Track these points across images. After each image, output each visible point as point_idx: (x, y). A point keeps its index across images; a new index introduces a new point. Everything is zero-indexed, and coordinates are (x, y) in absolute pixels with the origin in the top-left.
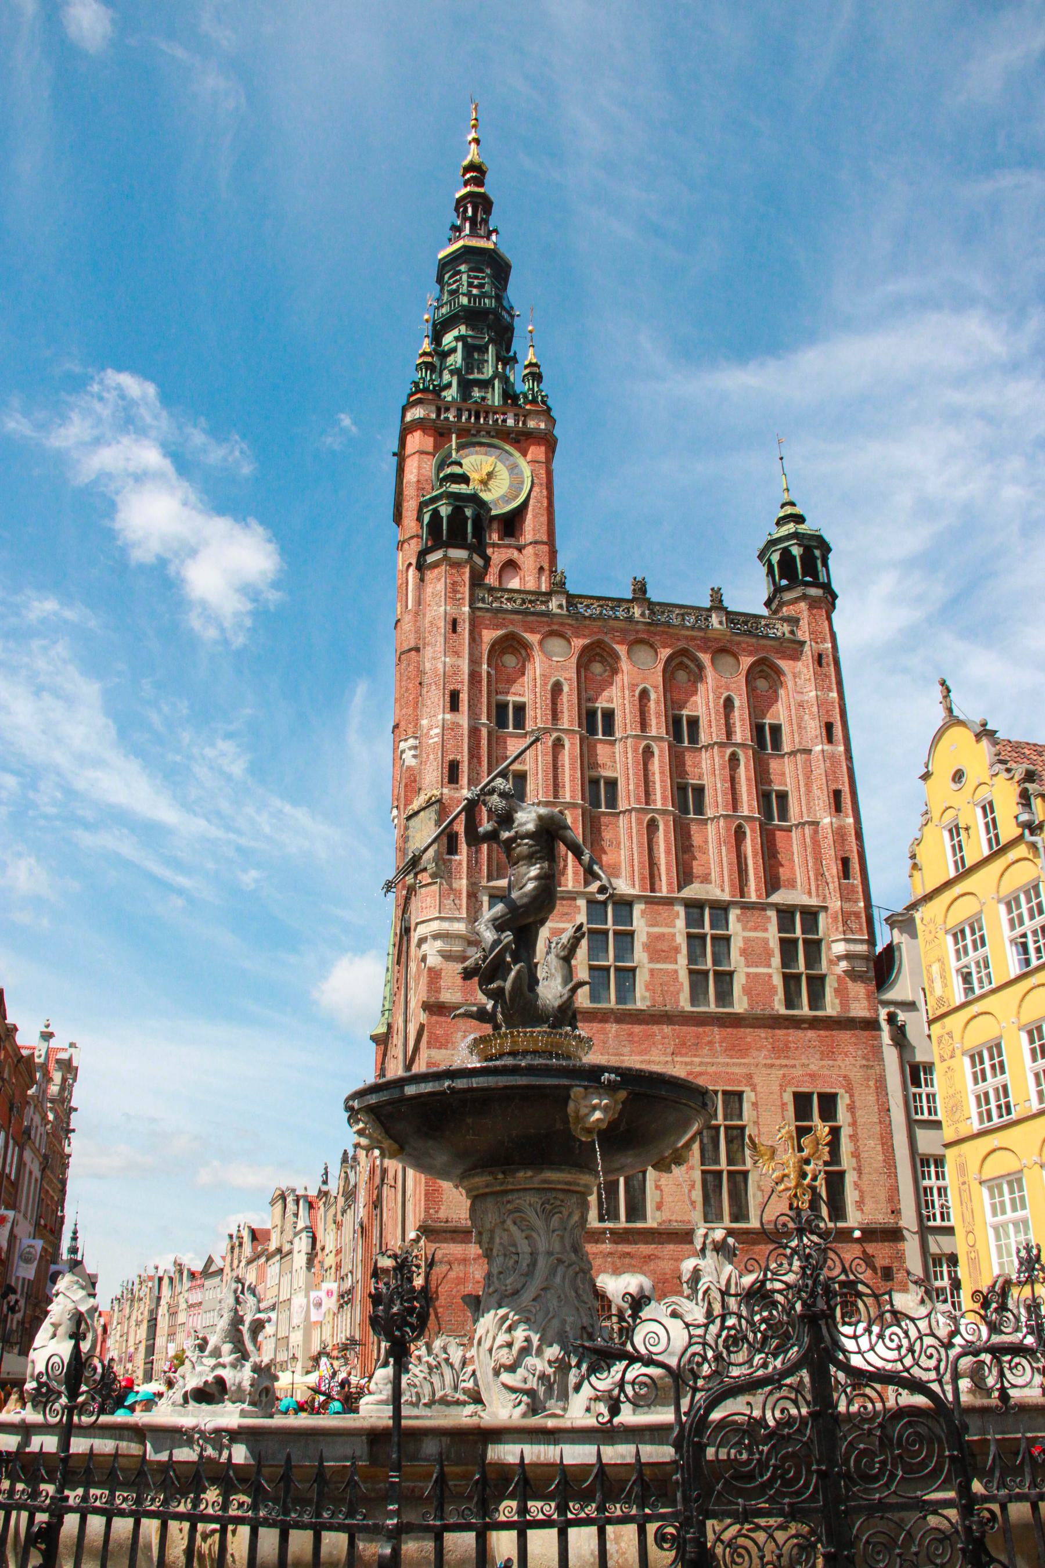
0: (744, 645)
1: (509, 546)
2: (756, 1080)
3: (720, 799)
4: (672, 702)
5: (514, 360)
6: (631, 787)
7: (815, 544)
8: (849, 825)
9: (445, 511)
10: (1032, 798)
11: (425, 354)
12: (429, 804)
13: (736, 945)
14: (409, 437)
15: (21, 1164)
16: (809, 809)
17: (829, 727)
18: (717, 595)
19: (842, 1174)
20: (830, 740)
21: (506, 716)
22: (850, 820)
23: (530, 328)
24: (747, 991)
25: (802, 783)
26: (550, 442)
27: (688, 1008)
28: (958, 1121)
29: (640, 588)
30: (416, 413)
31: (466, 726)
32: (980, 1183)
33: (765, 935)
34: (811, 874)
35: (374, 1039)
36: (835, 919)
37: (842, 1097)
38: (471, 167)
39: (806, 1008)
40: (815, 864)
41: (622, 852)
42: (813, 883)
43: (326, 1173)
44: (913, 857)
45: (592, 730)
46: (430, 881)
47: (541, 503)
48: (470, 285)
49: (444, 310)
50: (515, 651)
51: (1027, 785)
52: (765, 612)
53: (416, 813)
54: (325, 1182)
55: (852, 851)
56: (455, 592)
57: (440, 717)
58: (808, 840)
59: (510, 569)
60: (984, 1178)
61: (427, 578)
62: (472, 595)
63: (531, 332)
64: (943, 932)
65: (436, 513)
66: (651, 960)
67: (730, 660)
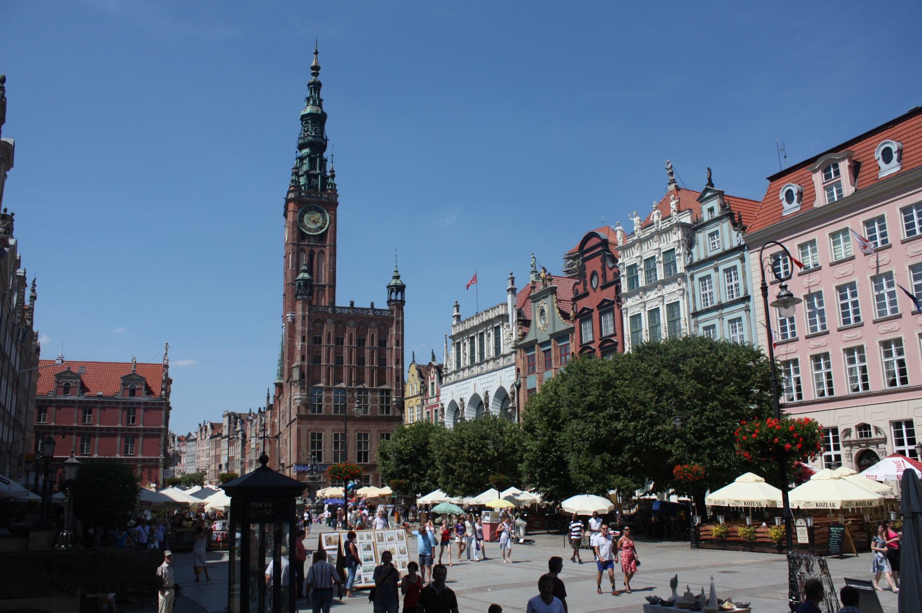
13: (369, 399)
18: (372, 304)
21: (318, 341)
29: (352, 303)
30: (291, 195)
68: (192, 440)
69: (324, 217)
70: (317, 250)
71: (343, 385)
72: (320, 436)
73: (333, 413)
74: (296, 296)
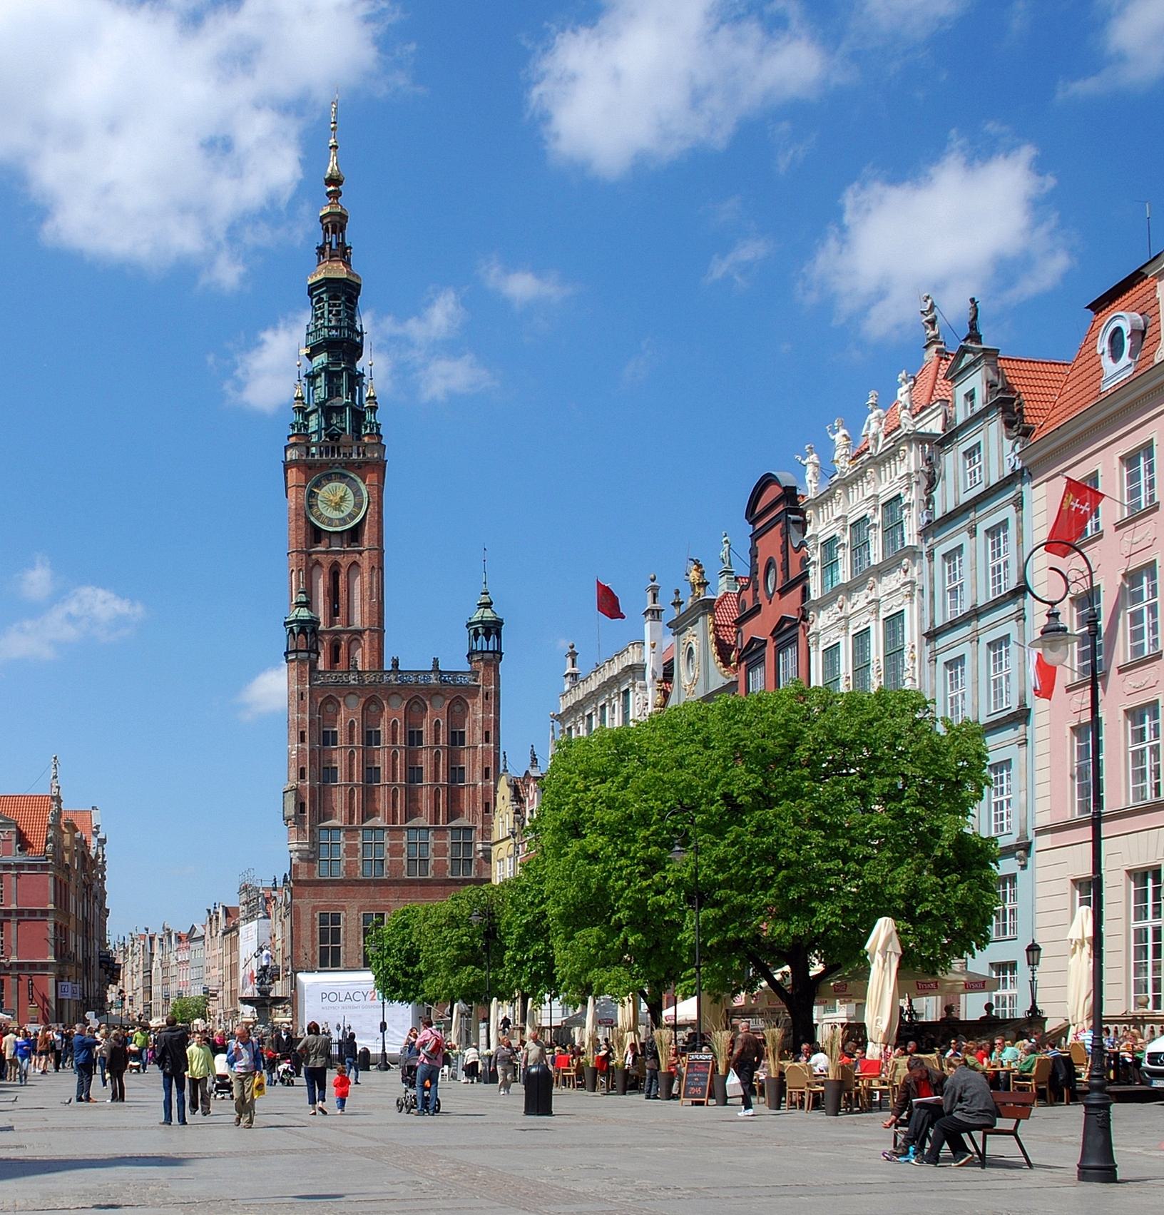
13: (431, 846)
18: (436, 660)
20: (487, 741)
21: (328, 738)
26: (379, 467)
29: (396, 663)
30: (293, 454)
65: (291, 630)
69: (357, 493)
70: (344, 561)
71: (379, 821)
72: (336, 919)
74: (286, 654)
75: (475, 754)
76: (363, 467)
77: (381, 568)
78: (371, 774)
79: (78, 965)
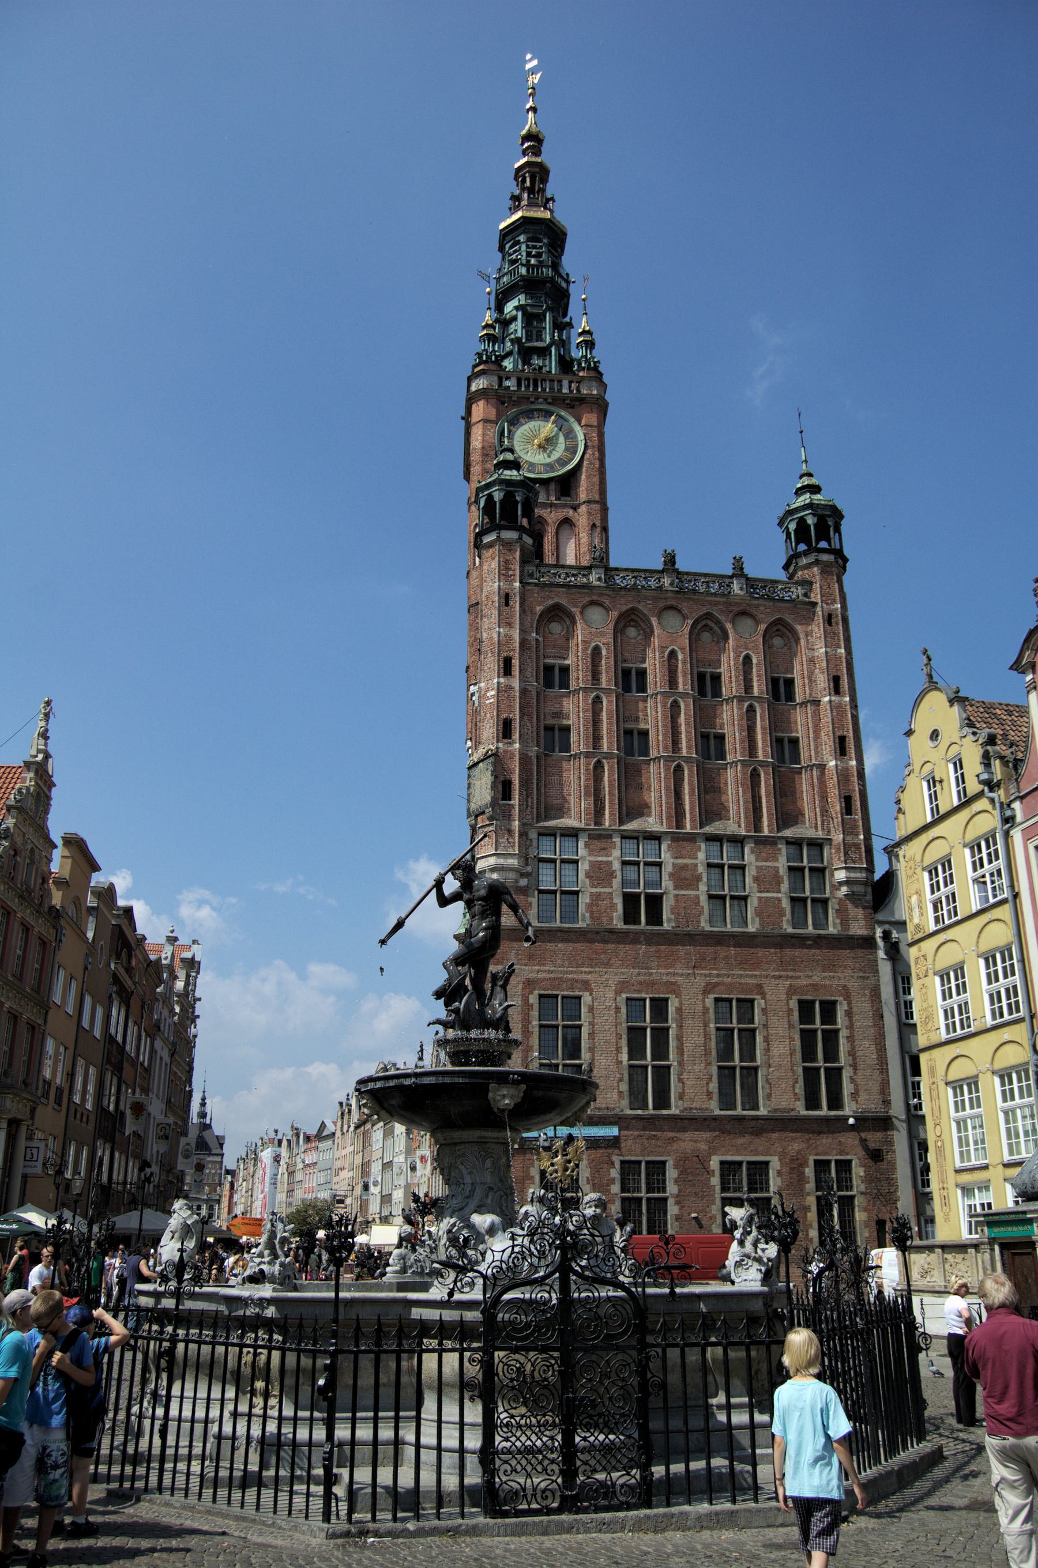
0: (762, 608)
1: (565, 506)
2: (767, 989)
3: (738, 746)
4: (698, 661)
5: (570, 325)
6: (660, 738)
7: (829, 513)
8: (852, 767)
9: (498, 496)
10: (992, 760)
11: (487, 326)
12: (486, 757)
13: (750, 873)
14: (474, 406)
15: (153, 1051)
16: (817, 753)
17: (836, 680)
18: (738, 564)
19: (840, 1069)
21: (555, 677)
22: (854, 763)
23: (583, 297)
24: (759, 913)
25: (811, 730)
26: (601, 407)
27: (708, 928)
28: (929, 1031)
29: (671, 559)
30: (479, 384)
31: (518, 688)
32: (946, 1084)
33: (776, 864)
34: (818, 810)
35: (456, 937)
36: (838, 850)
37: (841, 1004)
38: (529, 137)
39: (811, 928)
40: (821, 801)
41: (652, 794)
42: (819, 819)
43: (422, 1051)
44: (898, 802)
45: (627, 688)
46: (488, 823)
47: (594, 464)
48: (529, 254)
49: (505, 279)
50: (560, 620)
51: (989, 748)
52: (782, 576)
53: (475, 764)
54: (421, 1059)
55: (854, 790)
56: (510, 569)
57: (495, 681)
58: (815, 780)
59: (566, 526)
60: (950, 1078)
61: (483, 557)
62: (522, 571)
63: (584, 300)
64: (920, 869)
65: (490, 497)
66: (676, 888)
67: (749, 622)
68: (327, 1137)
69: (570, 435)
70: (552, 517)
73: (618, 924)
75: (816, 714)
76: (575, 404)
77: (605, 529)
78: (634, 740)
79: (76, 1112)
